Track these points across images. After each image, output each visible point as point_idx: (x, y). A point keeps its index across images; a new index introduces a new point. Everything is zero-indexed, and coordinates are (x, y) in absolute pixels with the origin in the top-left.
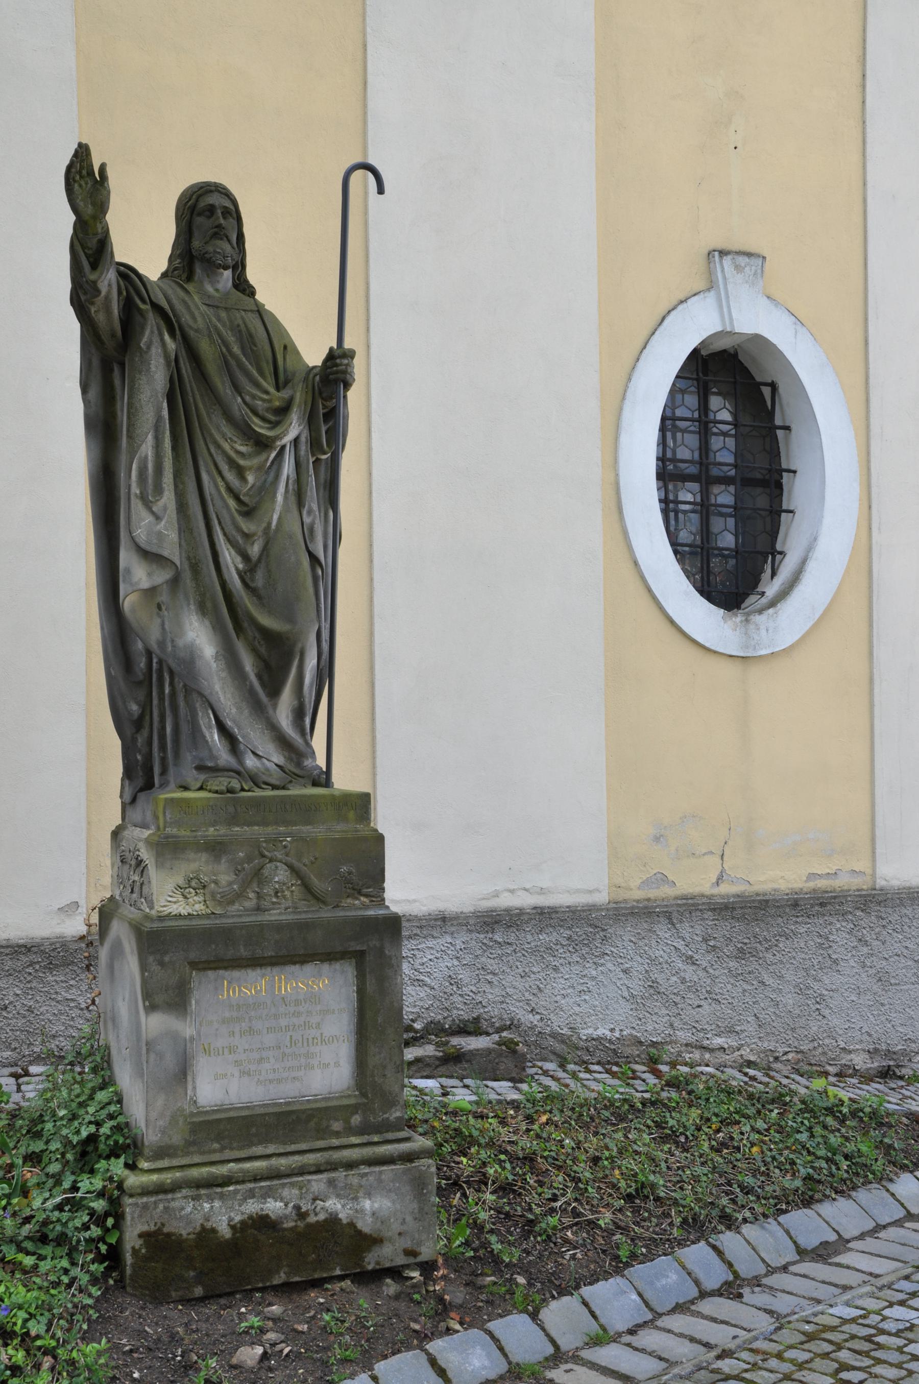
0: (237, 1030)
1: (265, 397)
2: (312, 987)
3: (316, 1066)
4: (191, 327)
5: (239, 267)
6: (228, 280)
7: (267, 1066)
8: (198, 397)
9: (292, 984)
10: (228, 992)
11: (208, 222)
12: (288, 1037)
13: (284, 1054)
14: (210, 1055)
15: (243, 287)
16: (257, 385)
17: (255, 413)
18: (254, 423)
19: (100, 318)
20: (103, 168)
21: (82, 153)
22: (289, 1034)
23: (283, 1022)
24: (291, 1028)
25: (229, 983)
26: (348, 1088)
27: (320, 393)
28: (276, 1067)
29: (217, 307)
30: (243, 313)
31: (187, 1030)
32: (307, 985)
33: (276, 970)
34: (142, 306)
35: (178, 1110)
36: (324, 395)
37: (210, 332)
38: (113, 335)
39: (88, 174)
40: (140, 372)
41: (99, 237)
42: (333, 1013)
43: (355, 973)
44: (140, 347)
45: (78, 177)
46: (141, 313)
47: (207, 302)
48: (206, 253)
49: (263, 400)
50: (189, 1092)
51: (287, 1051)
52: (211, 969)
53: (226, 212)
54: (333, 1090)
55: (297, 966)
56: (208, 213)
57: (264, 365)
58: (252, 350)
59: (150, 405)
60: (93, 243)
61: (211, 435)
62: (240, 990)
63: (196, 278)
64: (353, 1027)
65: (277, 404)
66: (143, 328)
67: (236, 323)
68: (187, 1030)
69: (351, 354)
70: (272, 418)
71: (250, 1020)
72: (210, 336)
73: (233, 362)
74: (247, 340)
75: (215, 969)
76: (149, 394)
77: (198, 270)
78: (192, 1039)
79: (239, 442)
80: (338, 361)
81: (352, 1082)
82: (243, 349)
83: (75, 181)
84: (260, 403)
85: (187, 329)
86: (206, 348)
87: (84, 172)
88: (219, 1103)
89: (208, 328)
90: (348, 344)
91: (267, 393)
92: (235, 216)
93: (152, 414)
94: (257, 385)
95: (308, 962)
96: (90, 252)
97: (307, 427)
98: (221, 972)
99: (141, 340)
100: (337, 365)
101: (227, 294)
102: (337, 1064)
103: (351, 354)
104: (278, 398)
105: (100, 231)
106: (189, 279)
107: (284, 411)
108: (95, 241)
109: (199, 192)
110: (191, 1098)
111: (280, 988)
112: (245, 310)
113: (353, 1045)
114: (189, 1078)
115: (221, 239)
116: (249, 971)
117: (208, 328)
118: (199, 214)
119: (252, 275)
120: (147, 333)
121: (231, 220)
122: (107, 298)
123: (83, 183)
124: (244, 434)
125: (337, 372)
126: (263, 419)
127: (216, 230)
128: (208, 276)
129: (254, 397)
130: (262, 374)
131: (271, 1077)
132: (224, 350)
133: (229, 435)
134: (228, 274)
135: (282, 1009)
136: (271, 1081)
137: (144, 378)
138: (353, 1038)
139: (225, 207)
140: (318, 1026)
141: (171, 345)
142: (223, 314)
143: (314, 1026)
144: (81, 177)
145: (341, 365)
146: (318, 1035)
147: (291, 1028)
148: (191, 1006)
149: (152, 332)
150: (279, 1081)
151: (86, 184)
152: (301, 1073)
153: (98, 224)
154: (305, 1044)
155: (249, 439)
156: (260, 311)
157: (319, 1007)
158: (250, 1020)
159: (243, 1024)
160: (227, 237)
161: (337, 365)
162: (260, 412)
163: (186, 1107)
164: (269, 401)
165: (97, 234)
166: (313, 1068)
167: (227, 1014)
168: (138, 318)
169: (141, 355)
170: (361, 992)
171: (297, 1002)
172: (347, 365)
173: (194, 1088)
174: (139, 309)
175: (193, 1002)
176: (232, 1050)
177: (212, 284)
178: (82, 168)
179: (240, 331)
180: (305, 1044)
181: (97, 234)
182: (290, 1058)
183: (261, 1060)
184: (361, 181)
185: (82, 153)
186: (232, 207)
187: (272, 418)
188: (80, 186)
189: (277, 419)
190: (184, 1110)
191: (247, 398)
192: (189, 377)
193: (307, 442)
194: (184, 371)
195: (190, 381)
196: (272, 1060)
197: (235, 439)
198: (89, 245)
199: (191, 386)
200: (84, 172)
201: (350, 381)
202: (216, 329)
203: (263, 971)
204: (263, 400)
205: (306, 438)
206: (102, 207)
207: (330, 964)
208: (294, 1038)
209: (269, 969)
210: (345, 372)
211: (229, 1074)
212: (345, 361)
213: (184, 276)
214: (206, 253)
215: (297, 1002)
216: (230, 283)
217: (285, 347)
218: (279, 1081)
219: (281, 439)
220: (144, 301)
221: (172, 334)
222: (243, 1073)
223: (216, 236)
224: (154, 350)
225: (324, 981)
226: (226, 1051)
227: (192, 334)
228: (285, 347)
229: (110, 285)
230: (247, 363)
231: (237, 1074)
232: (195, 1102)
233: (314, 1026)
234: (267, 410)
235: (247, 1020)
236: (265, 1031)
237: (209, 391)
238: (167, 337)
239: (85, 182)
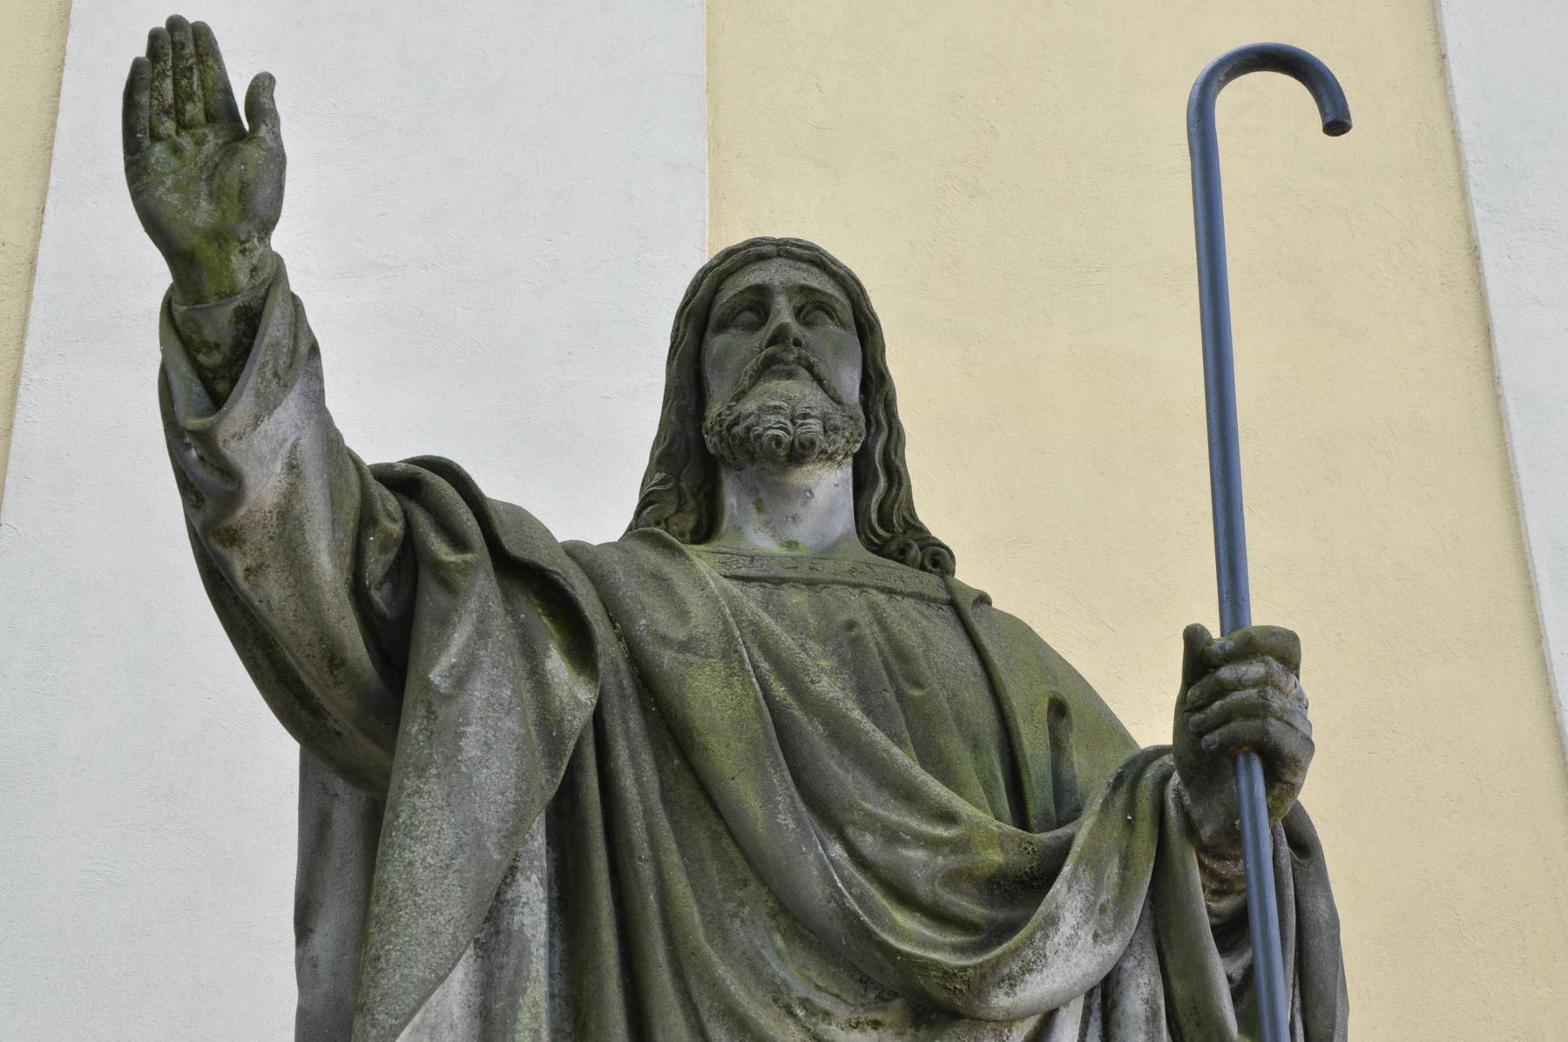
1: (940, 831)
4: (665, 641)
5: (878, 470)
6: (831, 512)
8: (673, 858)
11: (768, 357)
15: (891, 529)
16: (909, 795)
17: (904, 897)
18: (894, 929)
19: (272, 594)
20: (262, 87)
21: (179, 54)
27: (1191, 829)
29: (779, 582)
30: (881, 598)
34: (442, 551)
36: (1207, 832)
37: (731, 639)
38: (334, 660)
39: (210, 118)
40: (421, 771)
41: (239, 301)
44: (428, 686)
45: (168, 126)
46: (446, 580)
47: (743, 571)
48: (736, 423)
49: (933, 844)
53: (811, 306)
56: (748, 317)
57: (955, 747)
58: (900, 695)
59: (452, 878)
60: (220, 324)
61: (715, 986)
63: (725, 525)
65: (996, 857)
66: (444, 622)
67: (843, 617)
69: (1282, 651)
70: (974, 909)
72: (729, 653)
73: (812, 730)
74: (889, 677)
76: (449, 842)
77: (732, 499)
79: (842, 1012)
80: (1226, 673)
82: (864, 694)
83: (156, 138)
84: (917, 854)
85: (651, 648)
86: (713, 699)
87: (194, 110)
89: (727, 631)
90: (1262, 614)
91: (948, 817)
92: (847, 314)
93: (457, 912)
94: (909, 795)
96: (211, 360)
97: (1151, 963)
99: (432, 661)
100: (1222, 690)
101: (828, 551)
103: (1282, 651)
104: (995, 842)
105: (243, 279)
106: (706, 530)
107: (1025, 887)
108: (227, 312)
109: (725, 265)
112: (882, 590)
115: (790, 375)
117: (727, 631)
118: (722, 327)
119: (935, 505)
120: (460, 637)
121: (832, 327)
122: (288, 515)
123: (186, 141)
124: (865, 981)
125: (1226, 718)
126: (939, 916)
127: (771, 349)
128: (760, 507)
129: (892, 835)
130: (947, 776)
132: (779, 690)
133: (799, 989)
134: (828, 486)
137: (434, 787)
139: (804, 290)
141: (573, 691)
142: (797, 599)
144: (182, 126)
145: (1239, 685)
149: (481, 634)
151: (199, 143)
153: (236, 260)
155: (884, 998)
156: (965, 610)
160: (810, 368)
161: (1222, 690)
162: (923, 890)
164: (958, 846)
165: (233, 293)
168: (431, 597)
169: (431, 714)
172: (1263, 682)
174: (437, 566)
177: (773, 527)
178: (182, 96)
179: (856, 642)
181: (233, 293)
184: (1265, 109)
185: (179, 54)
186: (829, 288)
187: (974, 909)
188: (176, 150)
189: (1001, 915)
191: (869, 844)
192: (644, 797)
193: (1152, 1018)
194: (627, 781)
195: (648, 812)
197: (823, 1002)
198: (209, 334)
199: (650, 829)
200: (194, 110)
201: (1290, 744)
202: (757, 630)
204: (933, 844)
205: (1150, 1003)
206: (255, 206)
210: (1260, 710)
212: (1254, 670)
213: (690, 522)
214: (736, 423)
216: (844, 520)
217: (1058, 709)
219: (1012, 982)
220: (458, 542)
221: (582, 651)
223: (769, 367)
224: (479, 690)
227: (667, 659)
228: (1058, 709)
229: (293, 467)
230: (879, 737)
234: (954, 879)
237: (726, 841)
238: (556, 664)
239: (195, 136)
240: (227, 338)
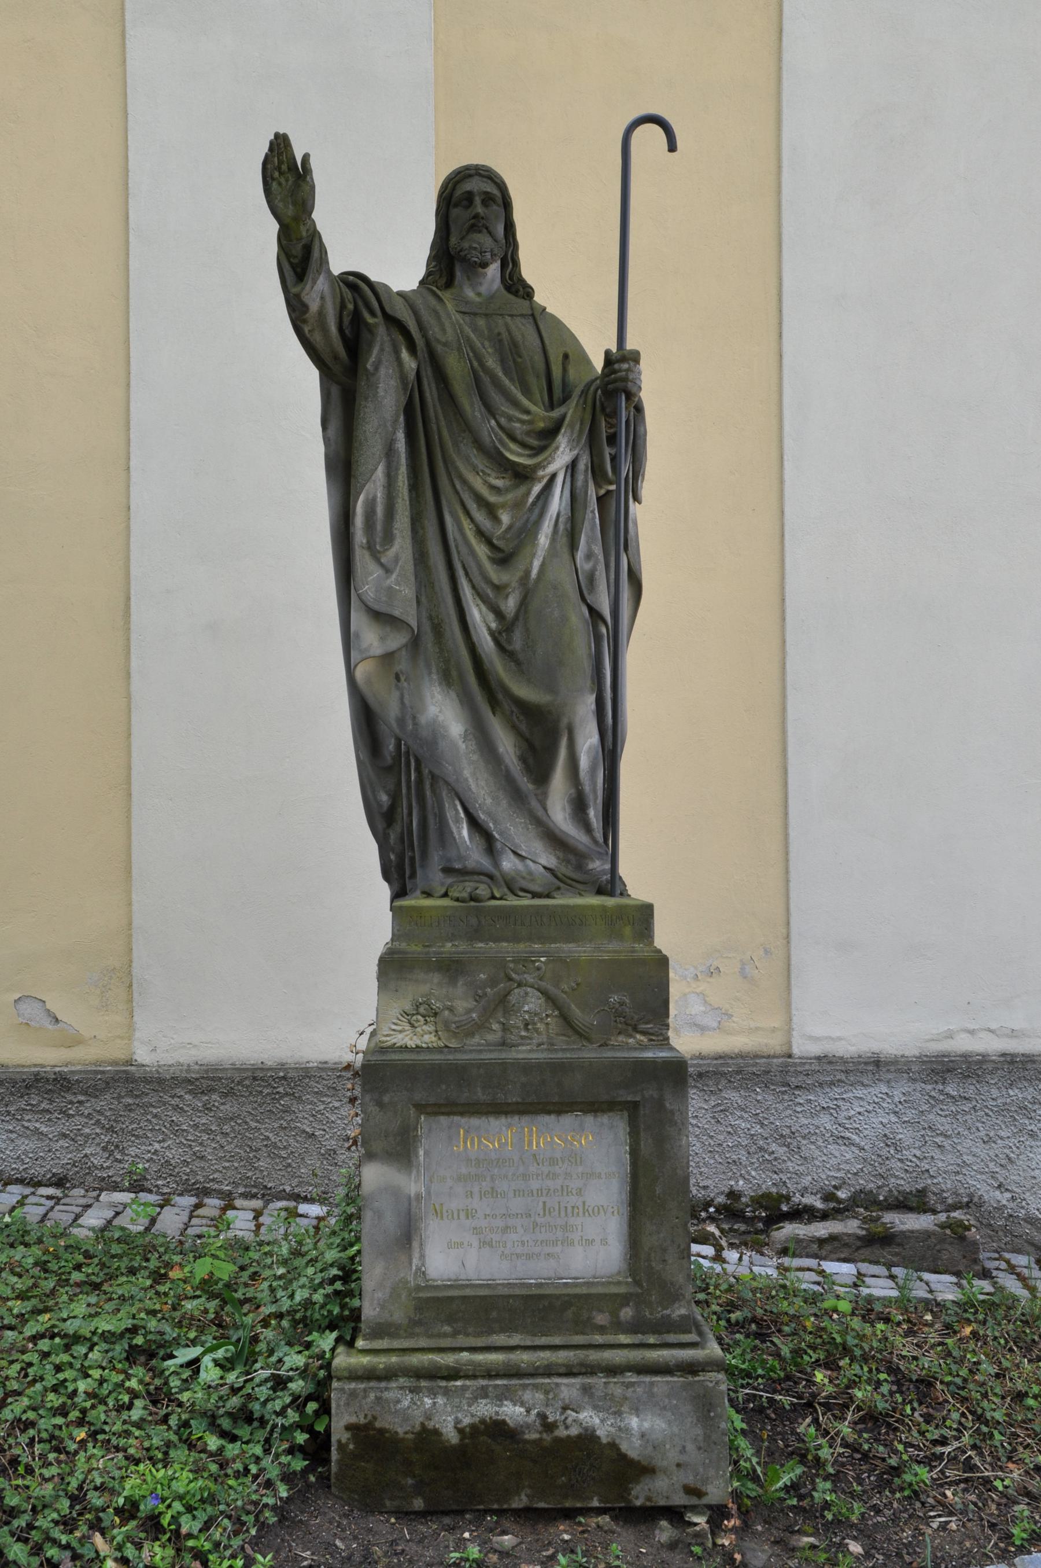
0: (476, 1190)
1: (525, 417)
2: (572, 1144)
3: (576, 1243)
4: (438, 341)
5: (510, 261)
6: (493, 281)
7: (514, 1237)
8: (443, 423)
9: (545, 1138)
10: (465, 1143)
11: (473, 214)
12: (541, 1204)
13: (535, 1224)
14: (442, 1218)
16: (515, 404)
17: (513, 438)
19: (317, 338)
20: (306, 158)
21: (280, 145)
22: (543, 1199)
23: (535, 1184)
24: (545, 1192)
25: (467, 1132)
26: (619, 1273)
27: (603, 409)
28: (525, 1239)
29: (475, 314)
30: (508, 319)
31: (412, 1185)
32: (565, 1141)
33: (526, 1119)
34: (370, 320)
35: (400, 1281)
36: (608, 410)
38: (336, 358)
39: (289, 169)
40: (366, 399)
41: (304, 242)
42: (599, 1176)
43: (628, 1130)
44: (366, 370)
45: (276, 174)
47: (463, 310)
48: (461, 251)
50: (415, 1261)
51: (539, 1220)
52: (443, 1114)
53: (488, 199)
54: (597, 1275)
55: (553, 1117)
56: (465, 203)
57: (532, 380)
58: (514, 360)
60: (297, 250)
61: (456, 468)
62: (480, 1142)
63: (456, 283)
64: (625, 1197)
65: (542, 425)
66: (370, 345)
67: (496, 331)
68: (412, 1185)
69: (634, 357)
70: (534, 442)
71: (493, 1179)
72: (459, 349)
73: (486, 379)
74: (510, 352)
75: (448, 1114)
78: (419, 1197)
79: (494, 474)
80: (616, 366)
81: (624, 1266)
82: (503, 361)
83: (273, 179)
84: (517, 425)
85: (434, 344)
86: (455, 366)
87: (284, 167)
88: (453, 1277)
90: (630, 345)
91: (527, 412)
92: (500, 201)
93: (380, 447)
94: (515, 404)
95: (567, 1112)
96: (295, 261)
97: (587, 452)
98: (457, 1118)
99: (367, 360)
100: (615, 372)
101: (492, 297)
102: (604, 1242)
103: (634, 357)
105: (304, 234)
106: (449, 284)
107: (550, 433)
108: (299, 246)
110: (418, 1269)
111: (530, 1143)
112: (511, 316)
113: (626, 1218)
114: (415, 1244)
115: (480, 232)
116: (492, 1119)
118: (456, 205)
119: (528, 272)
121: (495, 207)
122: (321, 313)
123: (282, 180)
125: (615, 381)
126: (524, 445)
127: (473, 221)
128: (469, 279)
129: (510, 419)
130: (526, 391)
131: (519, 1250)
132: (476, 364)
133: (481, 467)
134: (493, 270)
135: (533, 1169)
136: (518, 1256)
137: (370, 405)
138: (625, 1210)
140: (580, 1192)
141: (410, 363)
142: (481, 322)
143: (574, 1192)
144: (281, 173)
145: (620, 371)
146: (580, 1204)
147: (545, 1192)
148: (417, 1157)
149: (382, 350)
150: (529, 1257)
151: (287, 181)
152: (558, 1249)
153: (302, 227)
154: (563, 1214)
155: (506, 470)
156: (537, 316)
157: (580, 1169)
158: (493, 1179)
159: (484, 1184)
160: (487, 228)
161: (615, 372)
162: (519, 437)
163: (410, 1278)
165: (301, 239)
166: (572, 1244)
167: (464, 1170)
168: (365, 335)
170: (634, 1153)
171: (553, 1161)
172: (628, 370)
173: (422, 1257)
174: (367, 324)
175: (421, 1153)
176: (469, 1214)
177: (473, 287)
178: (280, 162)
179: (500, 341)
180: (563, 1214)
181: (301, 239)
182: (543, 1230)
183: (506, 1229)
184: (650, 136)
185: (280, 145)
186: (496, 192)
187: (534, 442)
188: (280, 184)
189: (542, 443)
190: (407, 1282)
191: (503, 421)
193: (586, 471)
194: (428, 395)
196: (520, 1230)
197: (488, 471)
198: (294, 252)
199: (435, 412)
200: (284, 167)
201: (634, 390)
203: (509, 1120)
205: (586, 465)
207: (595, 1116)
208: (548, 1206)
209: (516, 1118)
210: (625, 380)
211: (466, 1243)
212: (625, 366)
213: (444, 280)
214: (461, 251)
215: (553, 1161)
217: (566, 356)
218: (529, 1257)
219: (544, 467)
220: (373, 314)
221: (412, 349)
222: (484, 1243)
223: (473, 228)
224: (382, 371)
225: (587, 1138)
226: (462, 1215)
227: (439, 348)
228: (566, 356)
229: (322, 298)
231: (475, 1244)
232: (424, 1273)
233: (574, 1192)
234: (528, 433)
235: (488, 1179)
236: (511, 1194)
238: (405, 355)
239: (286, 178)
240: (300, 255)
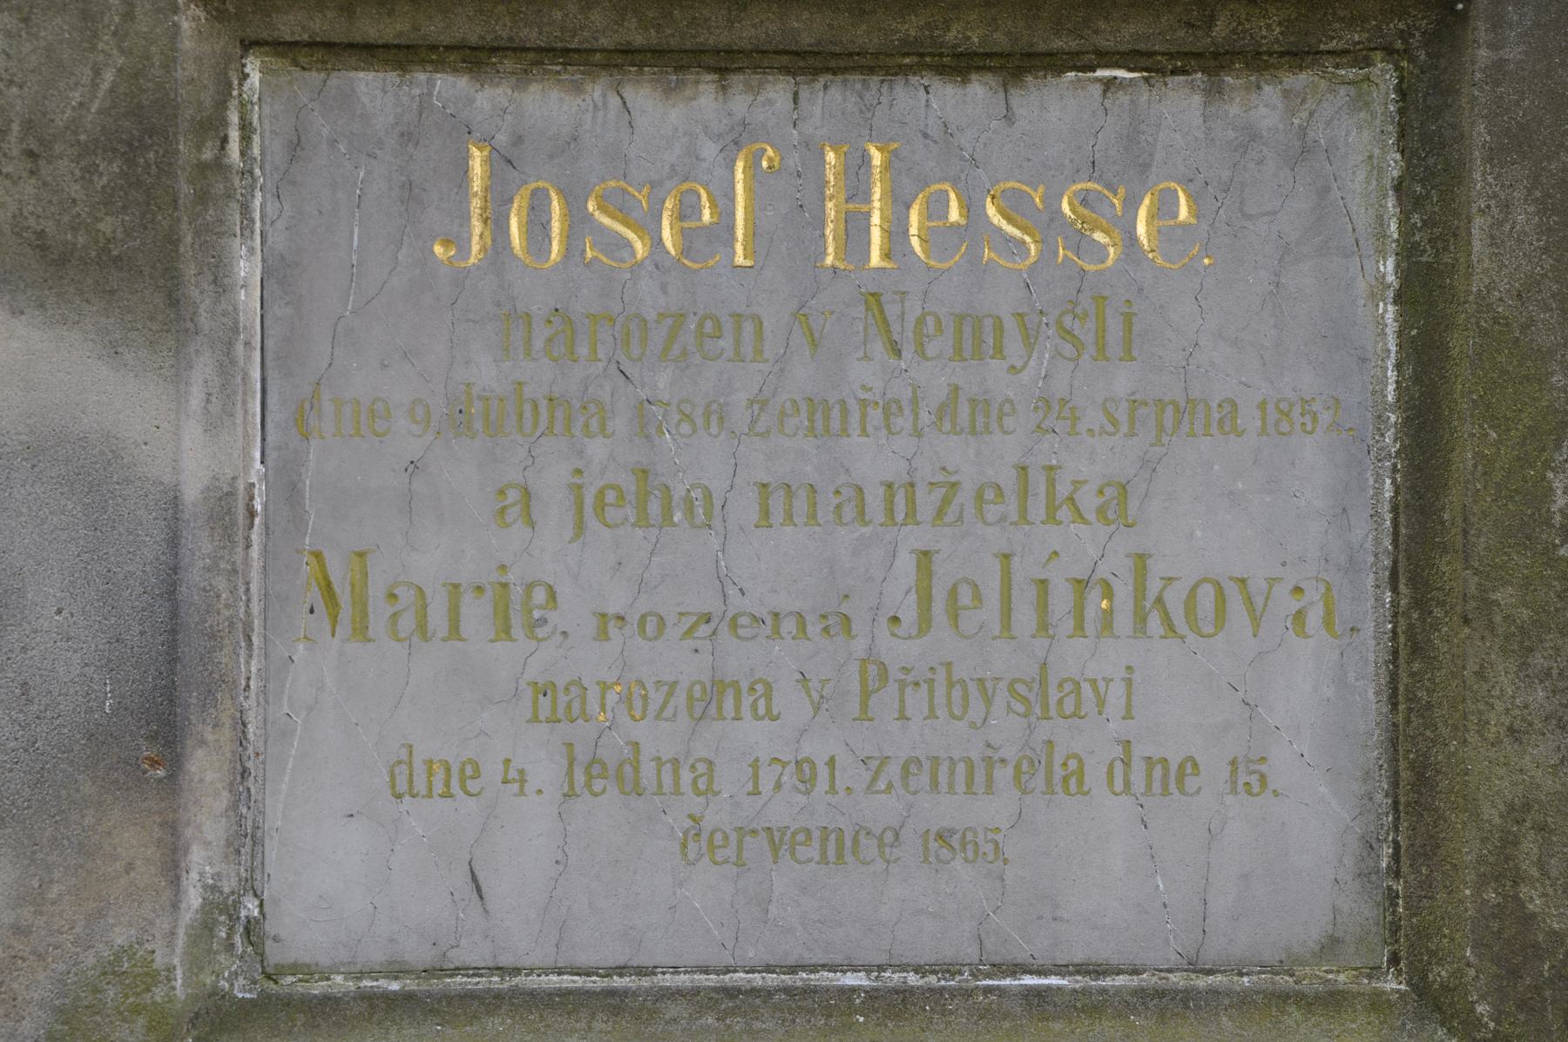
0: (553, 479)
2: (1080, 243)
3: (1095, 774)
7: (754, 735)
9: (936, 209)
10: (497, 224)
12: (906, 563)
13: (875, 672)
14: (361, 630)
22: (914, 538)
23: (873, 459)
24: (927, 502)
25: (505, 162)
26: (1331, 945)
28: (817, 749)
31: (183, 436)
32: (1048, 224)
33: (830, 100)
35: (110, 970)
42: (1228, 419)
43: (1394, 165)
50: (203, 863)
51: (899, 651)
52: (370, 53)
54: (1210, 956)
55: (979, 91)
62: (578, 222)
64: (1369, 535)
68: (183, 436)
71: (645, 425)
75: (402, 55)
78: (226, 510)
81: (1359, 910)
88: (417, 953)
95: (1053, 63)
98: (448, 86)
102: (1250, 775)
110: (220, 907)
111: (855, 229)
113: (1370, 648)
114: (205, 767)
116: (643, 96)
131: (782, 811)
135: (865, 373)
136: (779, 841)
138: (1368, 608)
140: (1118, 503)
143: (1088, 501)
146: (1117, 564)
147: (927, 502)
148: (221, 282)
150: (839, 846)
152: (995, 810)
154: (1025, 617)
157: (1123, 381)
158: (645, 425)
159: (597, 449)
163: (172, 956)
166: (1074, 780)
167: (486, 373)
170: (1425, 290)
171: (975, 335)
173: (246, 839)
175: (247, 267)
176: (516, 608)
180: (1025, 617)
182: (916, 701)
183: (712, 697)
190: (152, 977)
196: (792, 704)
203: (739, 102)
207: (1214, 92)
208: (944, 573)
209: (778, 91)
211: (492, 770)
215: (975, 335)
218: (839, 846)
222: (589, 771)
225: (1166, 207)
226: (475, 613)
231: (545, 772)
232: (252, 930)
233: (1088, 501)
235: (620, 424)
236: (745, 508)
